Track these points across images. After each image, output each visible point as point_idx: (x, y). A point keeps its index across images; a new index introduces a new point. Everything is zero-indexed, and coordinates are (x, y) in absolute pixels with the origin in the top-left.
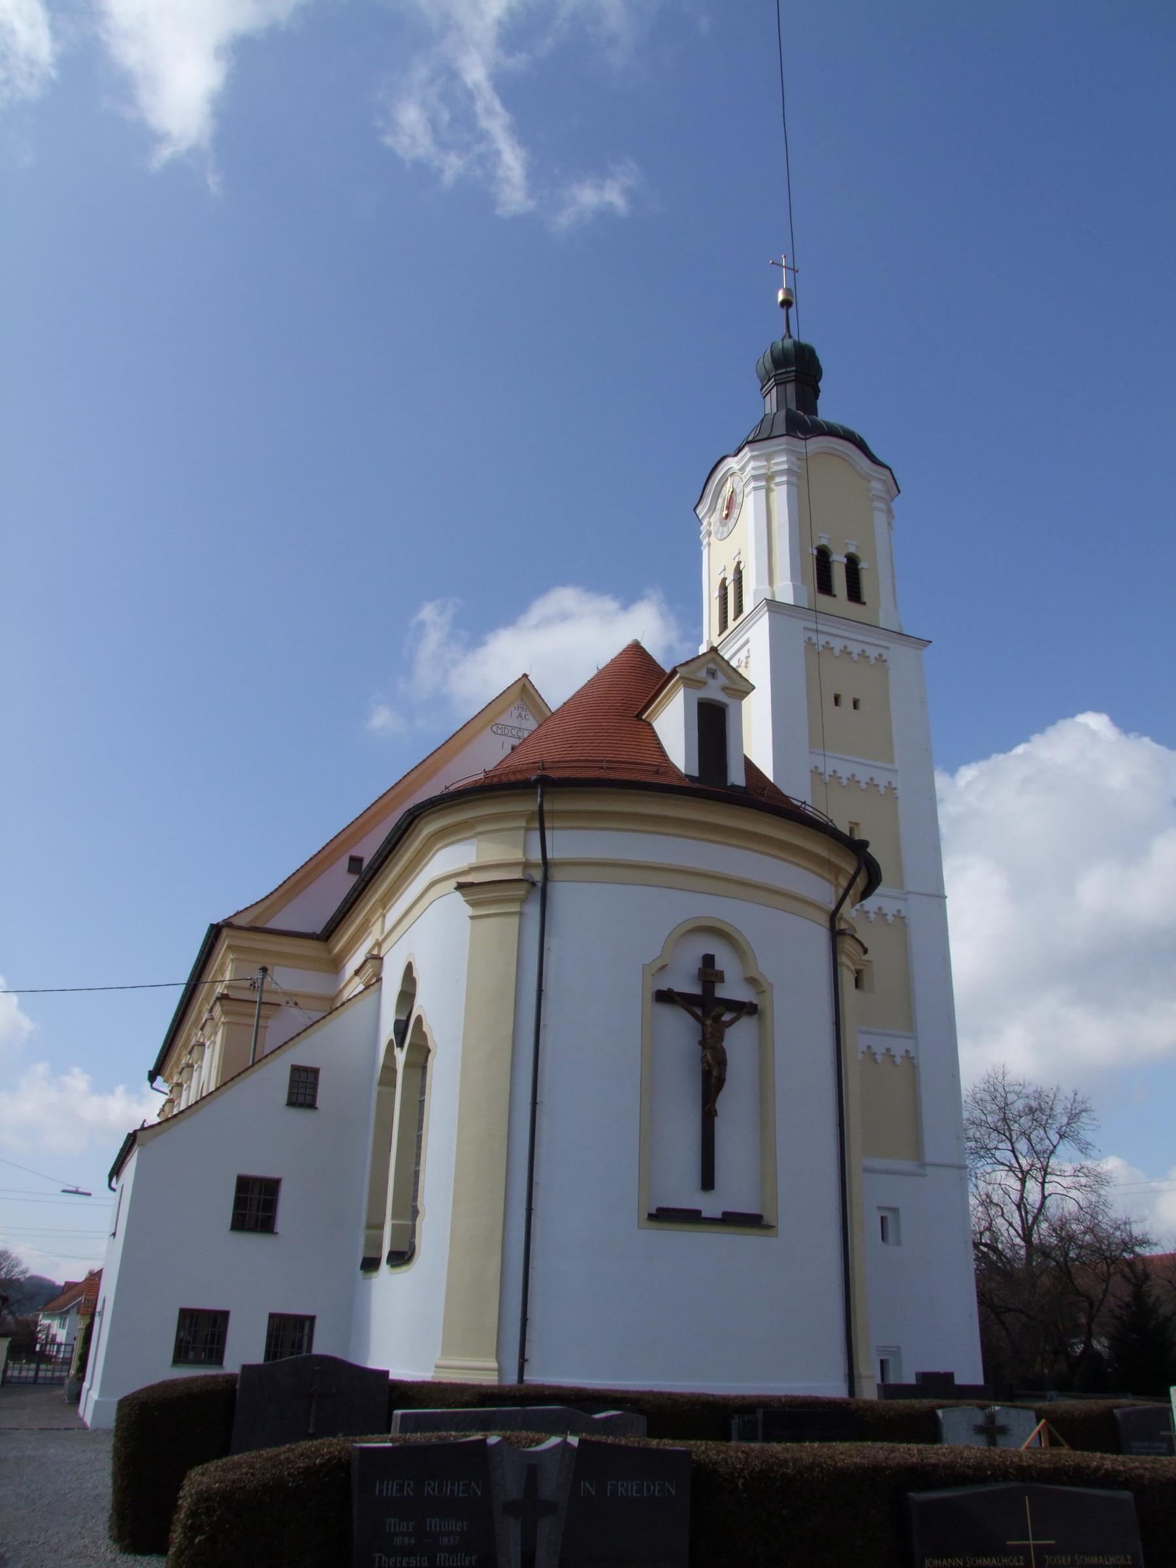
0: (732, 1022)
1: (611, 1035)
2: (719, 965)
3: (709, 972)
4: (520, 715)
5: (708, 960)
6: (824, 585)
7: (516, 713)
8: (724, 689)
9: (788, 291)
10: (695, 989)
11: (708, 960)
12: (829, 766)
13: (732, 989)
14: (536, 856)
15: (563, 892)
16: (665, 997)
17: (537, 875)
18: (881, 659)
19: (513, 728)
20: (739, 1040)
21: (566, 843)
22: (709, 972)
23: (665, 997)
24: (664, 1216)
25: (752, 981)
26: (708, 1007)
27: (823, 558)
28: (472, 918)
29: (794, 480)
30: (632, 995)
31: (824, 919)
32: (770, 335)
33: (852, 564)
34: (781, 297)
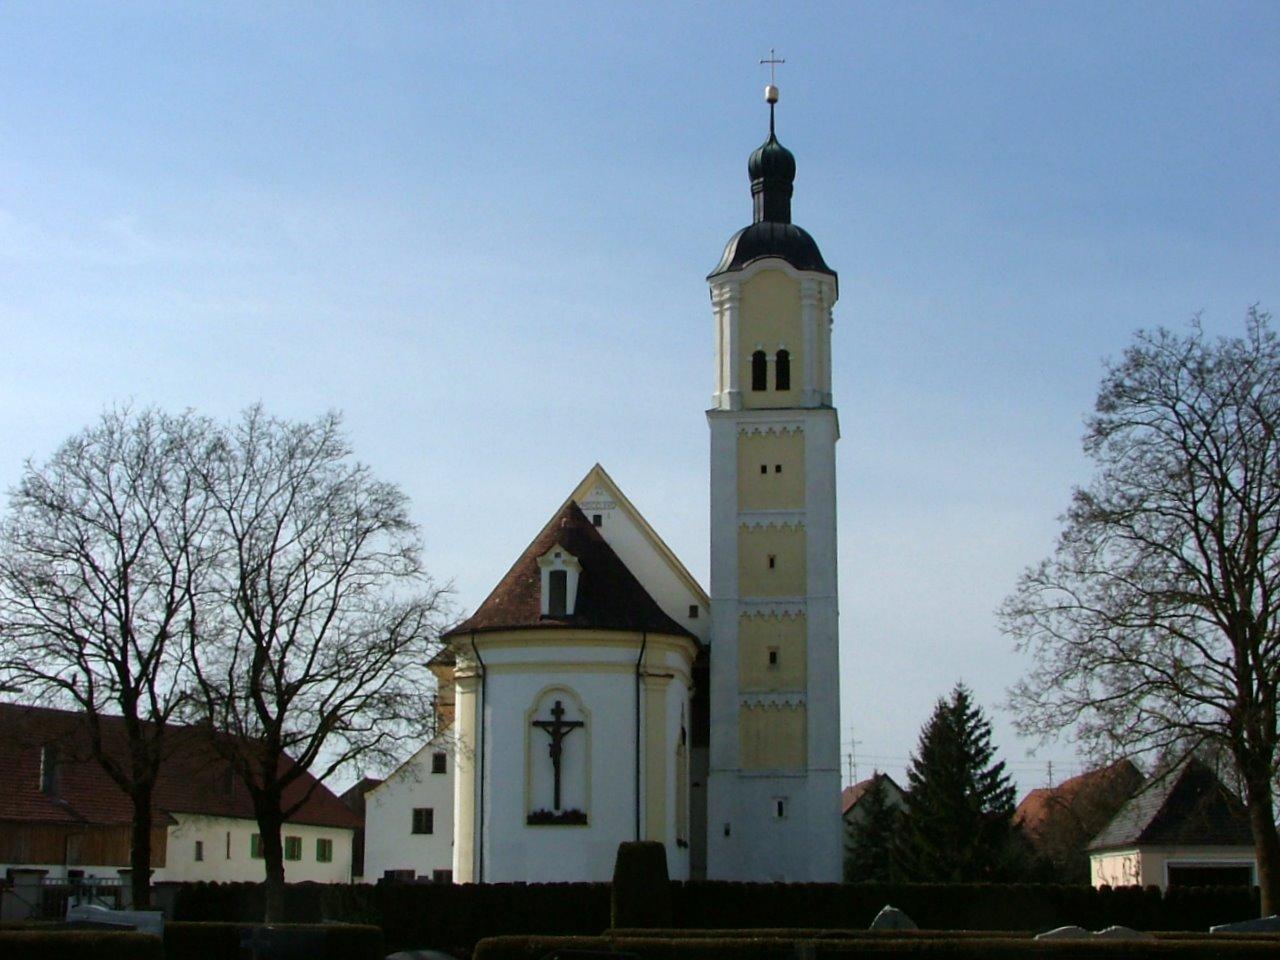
0: (567, 733)
1: (514, 741)
2: (562, 707)
3: (558, 710)
4: (597, 493)
5: (558, 704)
6: (759, 384)
7: (594, 492)
8: (564, 562)
9: (773, 90)
10: (551, 718)
11: (558, 704)
12: (751, 522)
13: (568, 717)
14: (480, 665)
15: (493, 679)
16: (536, 724)
17: (481, 672)
18: (799, 430)
19: (594, 503)
20: (573, 742)
21: (489, 656)
22: (558, 710)
23: (536, 724)
24: (537, 819)
25: (580, 710)
26: (557, 728)
27: (759, 359)
28: (462, 693)
29: (737, 304)
30: (520, 725)
31: (632, 670)
32: (753, 144)
33: (783, 358)
34: (767, 95)
